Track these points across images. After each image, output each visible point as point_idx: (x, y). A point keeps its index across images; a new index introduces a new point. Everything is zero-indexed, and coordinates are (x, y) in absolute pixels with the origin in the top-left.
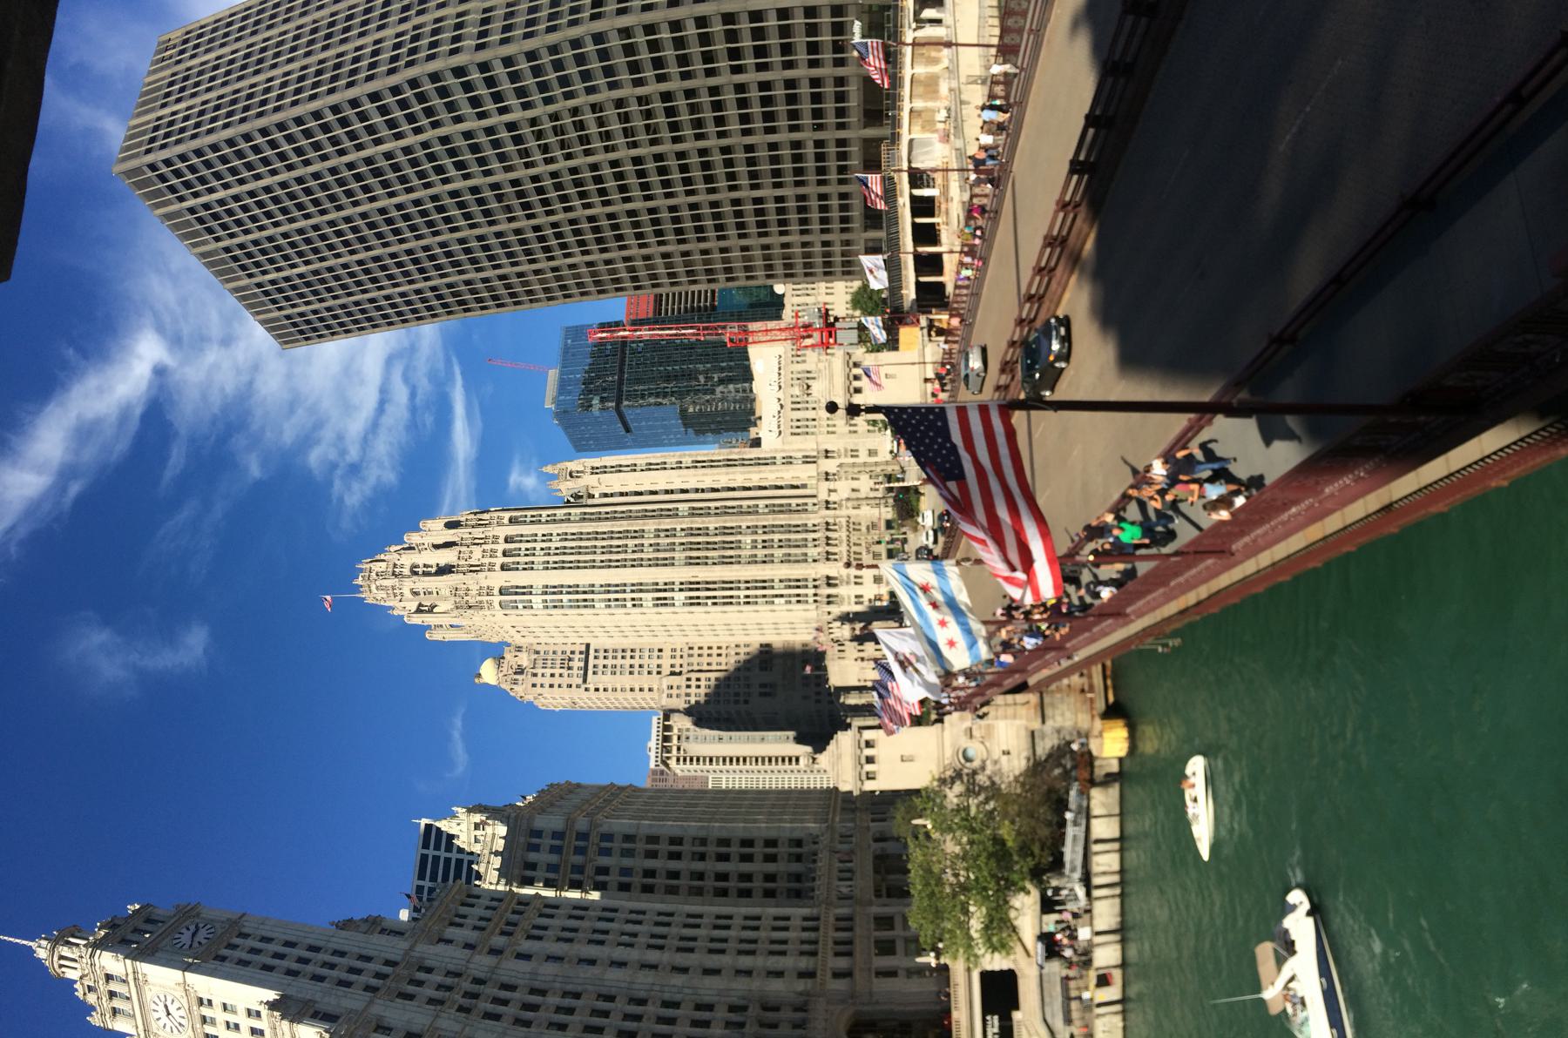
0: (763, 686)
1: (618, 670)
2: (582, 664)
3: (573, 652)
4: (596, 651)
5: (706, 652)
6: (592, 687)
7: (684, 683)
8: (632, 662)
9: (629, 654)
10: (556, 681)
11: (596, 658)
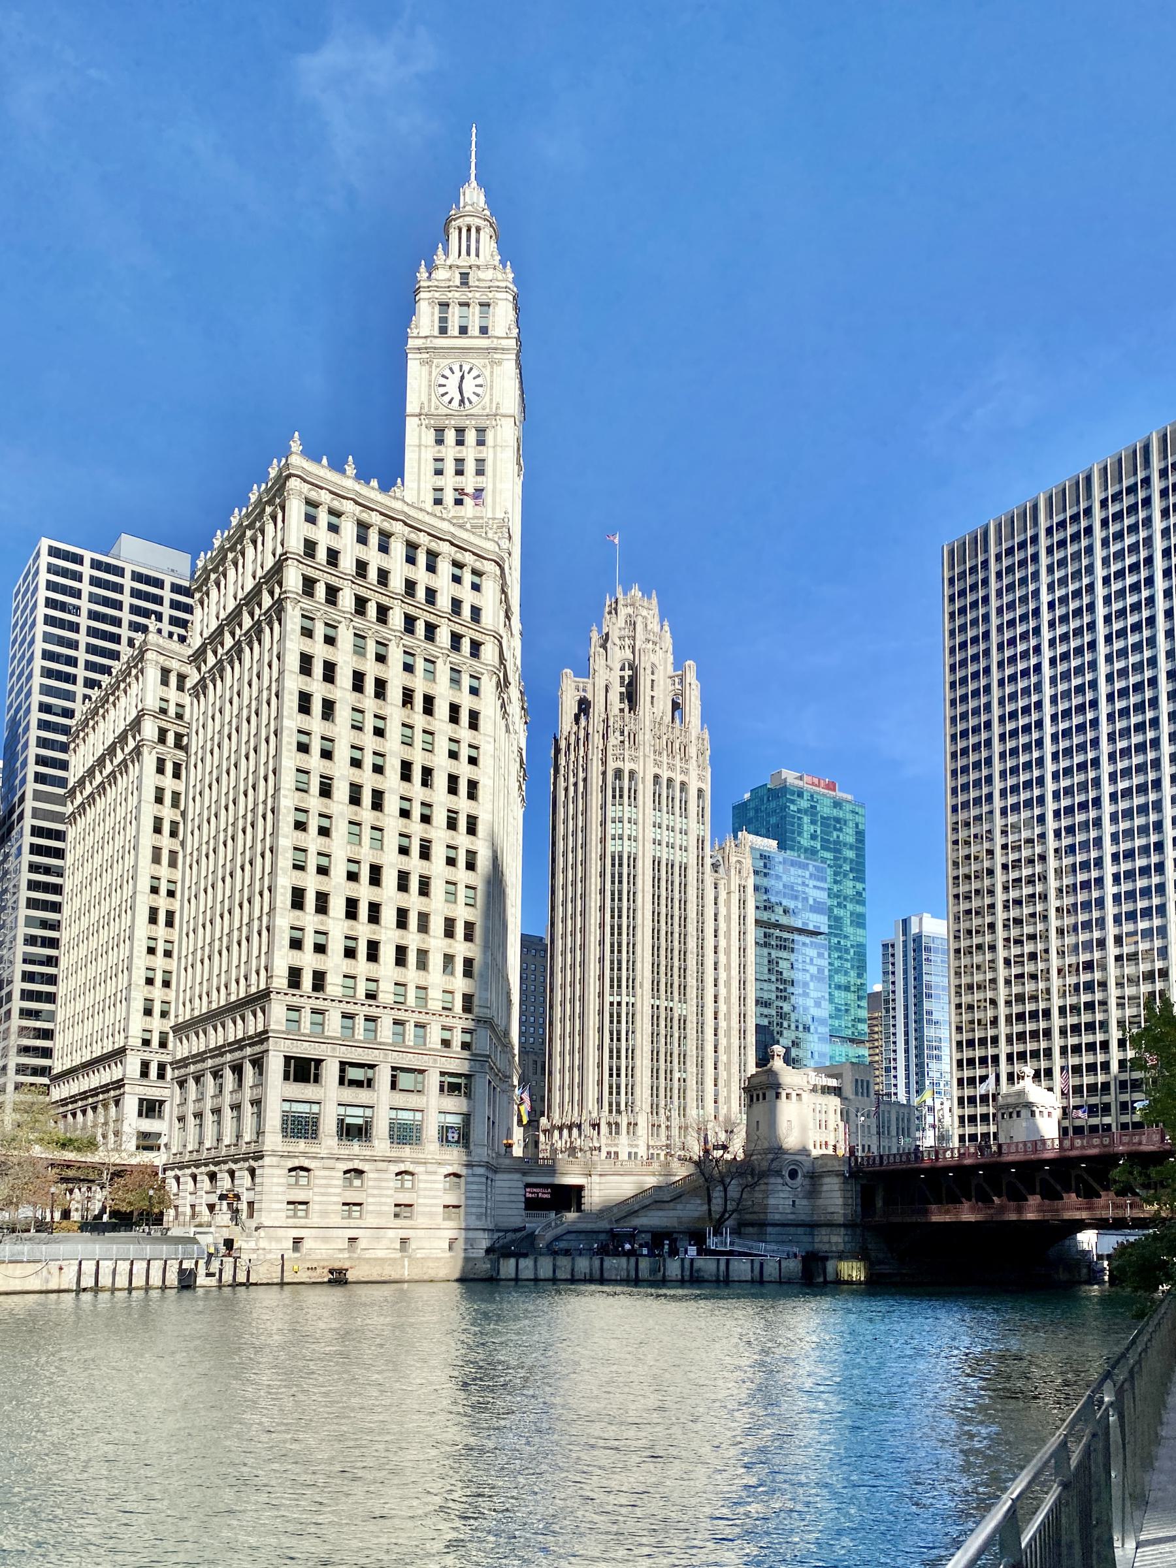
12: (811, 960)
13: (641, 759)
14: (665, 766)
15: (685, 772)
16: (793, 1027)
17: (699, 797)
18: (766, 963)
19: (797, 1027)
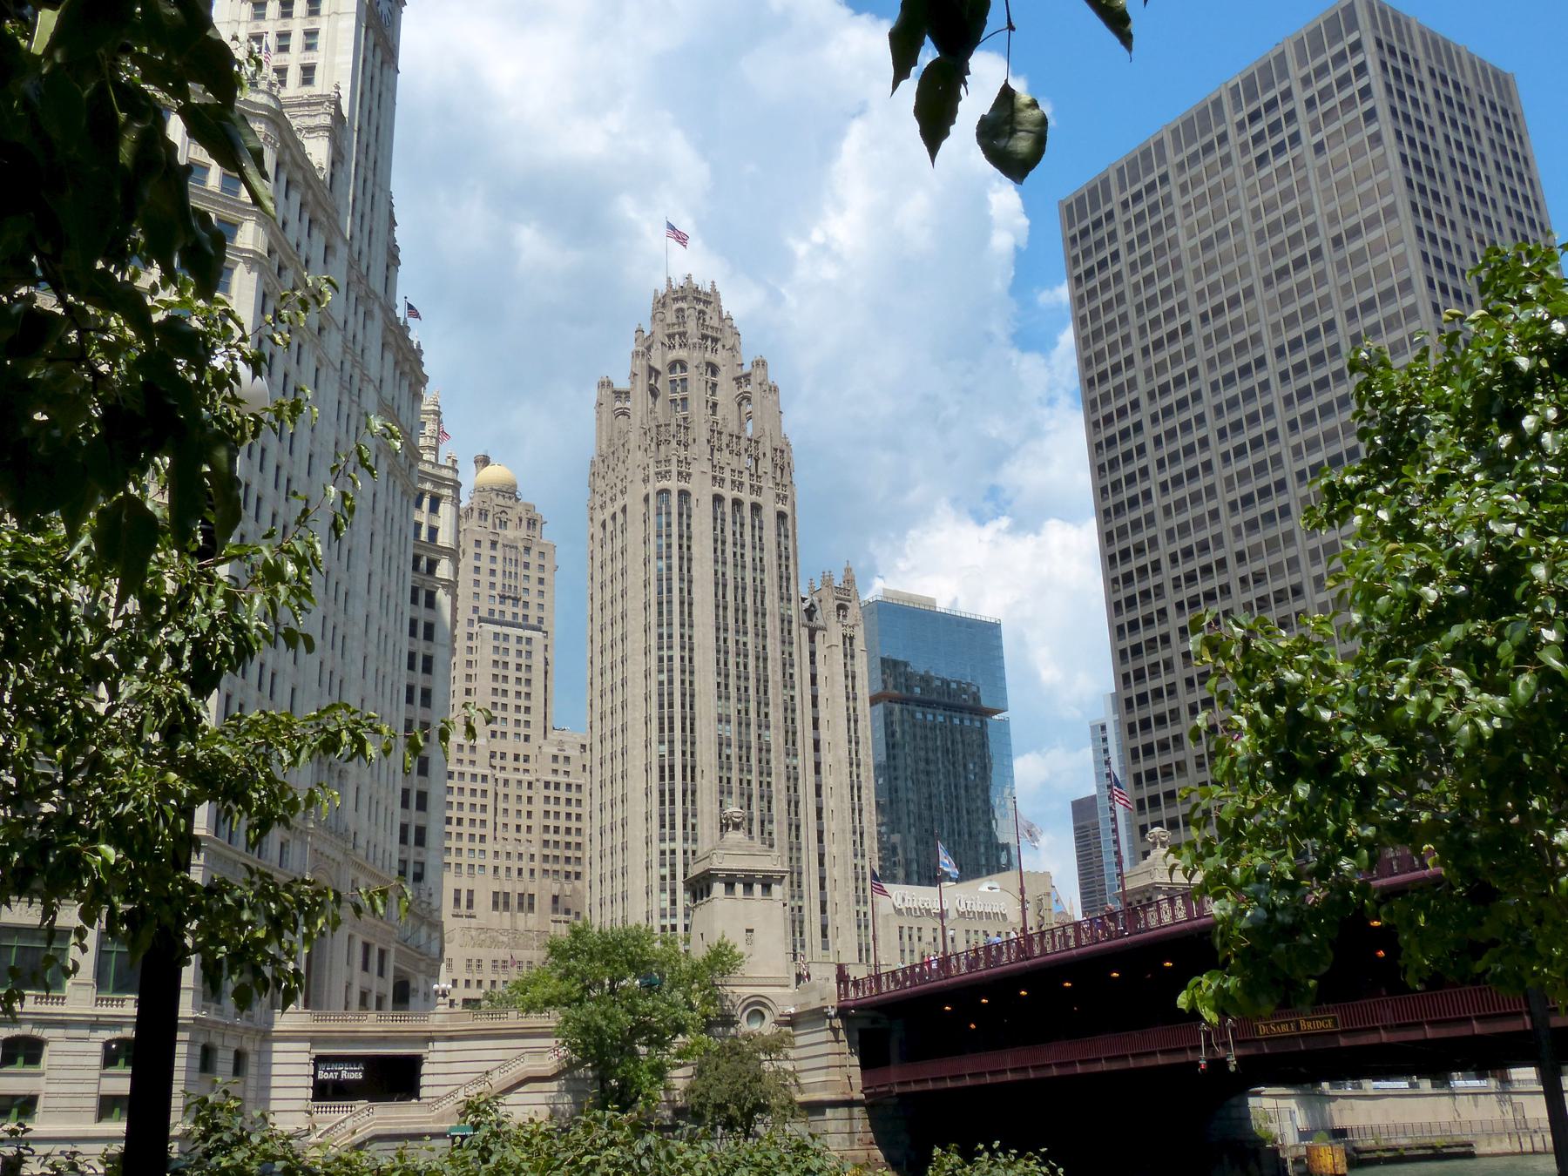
0: (470, 892)
1: (500, 671)
2: (508, 618)
3: (526, 604)
4: (529, 640)
5: (525, 807)
6: (476, 628)
7: (479, 770)
8: (511, 694)
9: (523, 689)
10: (485, 578)
11: (519, 639)
14: (728, 483)
15: (758, 490)
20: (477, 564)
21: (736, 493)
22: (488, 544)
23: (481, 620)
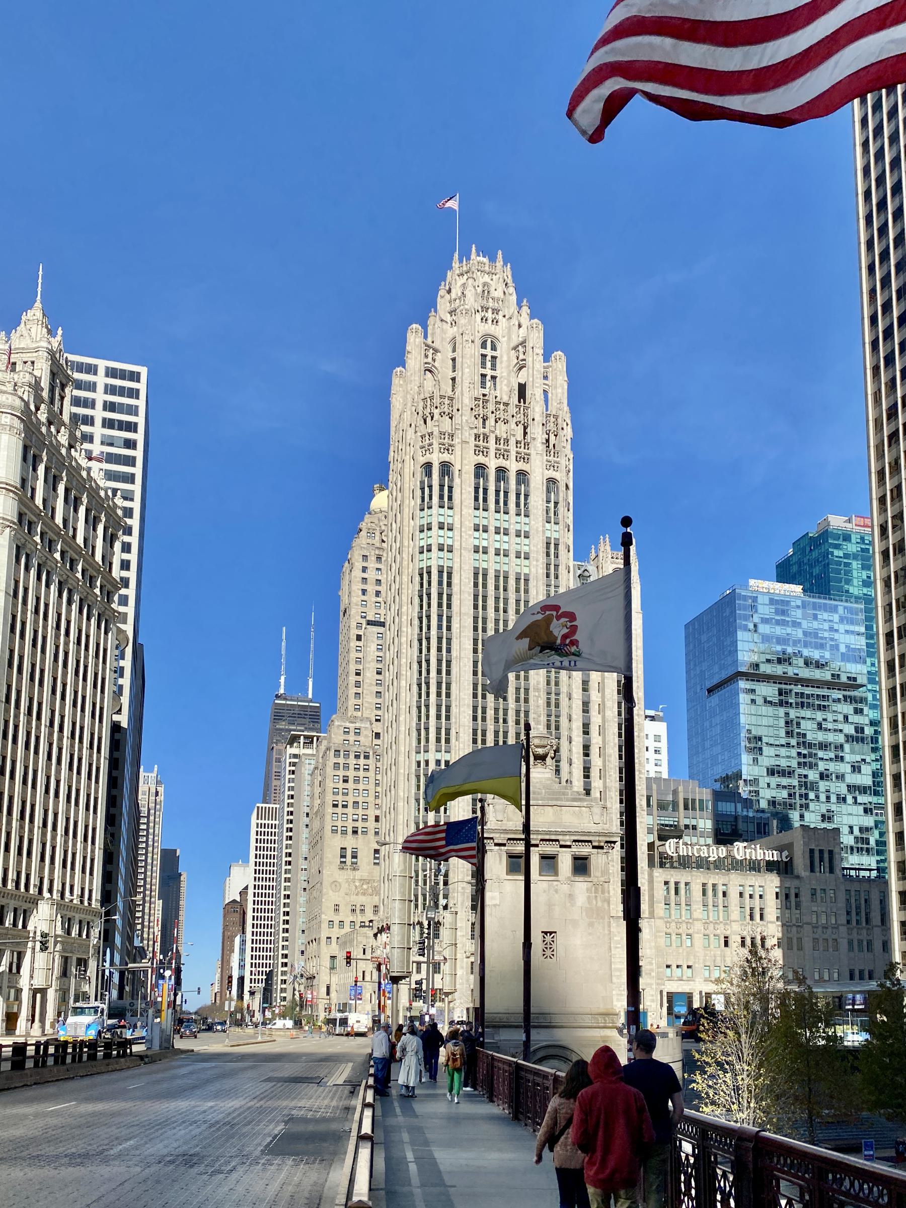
12: (846, 718)
13: (458, 449)
14: (492, 452)
15: (526, 459)
16: (823, 797)
17: (548, 491)
18: (782, 723)
19: (828, 798)
20: (365, 575)
21: (501, 462)
22: (374, 558)
23: (370, 623)
